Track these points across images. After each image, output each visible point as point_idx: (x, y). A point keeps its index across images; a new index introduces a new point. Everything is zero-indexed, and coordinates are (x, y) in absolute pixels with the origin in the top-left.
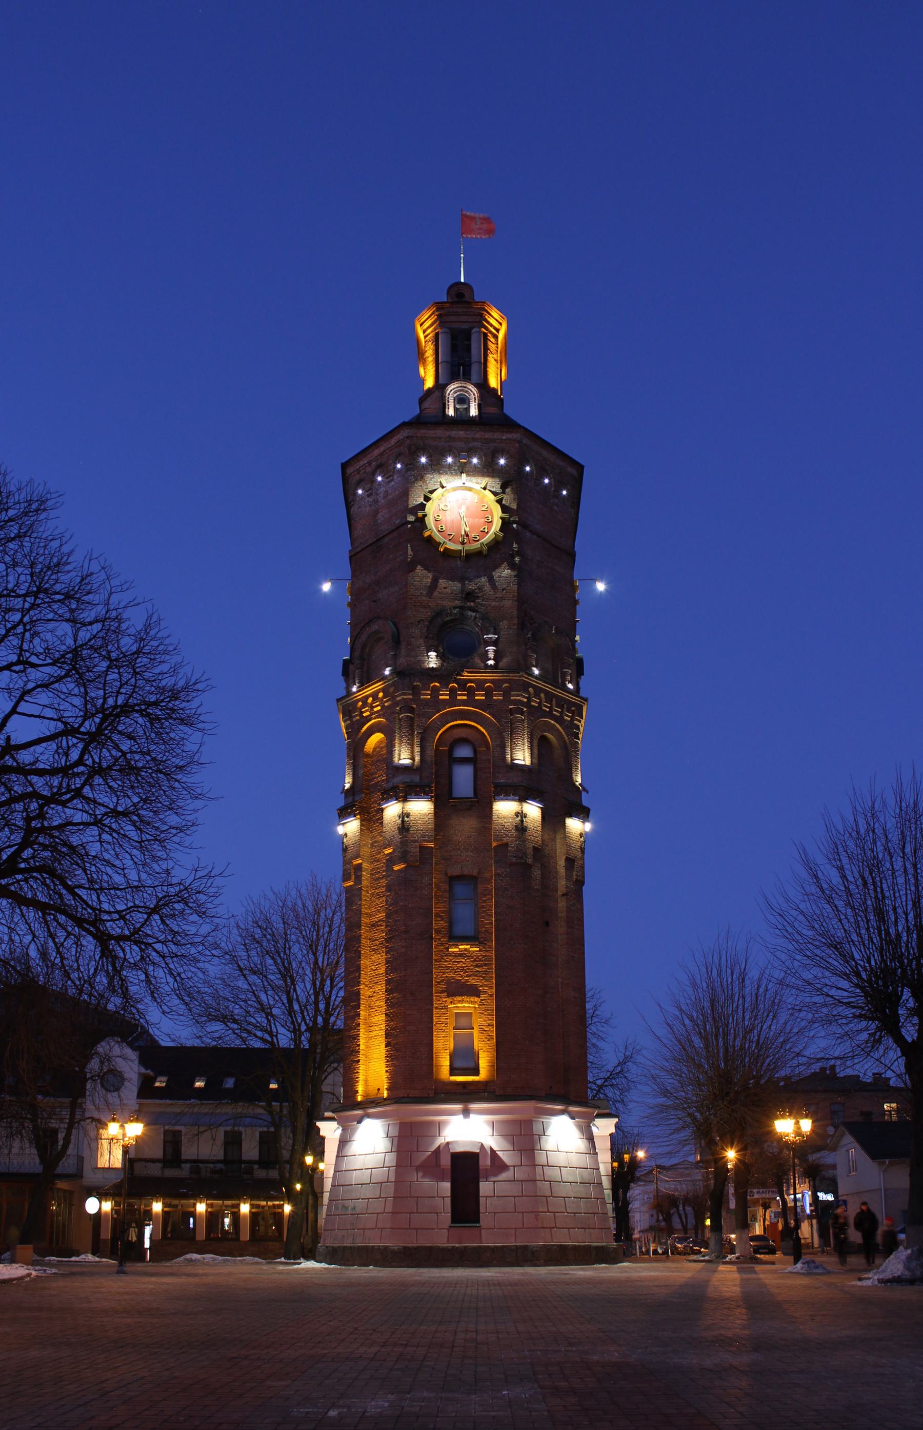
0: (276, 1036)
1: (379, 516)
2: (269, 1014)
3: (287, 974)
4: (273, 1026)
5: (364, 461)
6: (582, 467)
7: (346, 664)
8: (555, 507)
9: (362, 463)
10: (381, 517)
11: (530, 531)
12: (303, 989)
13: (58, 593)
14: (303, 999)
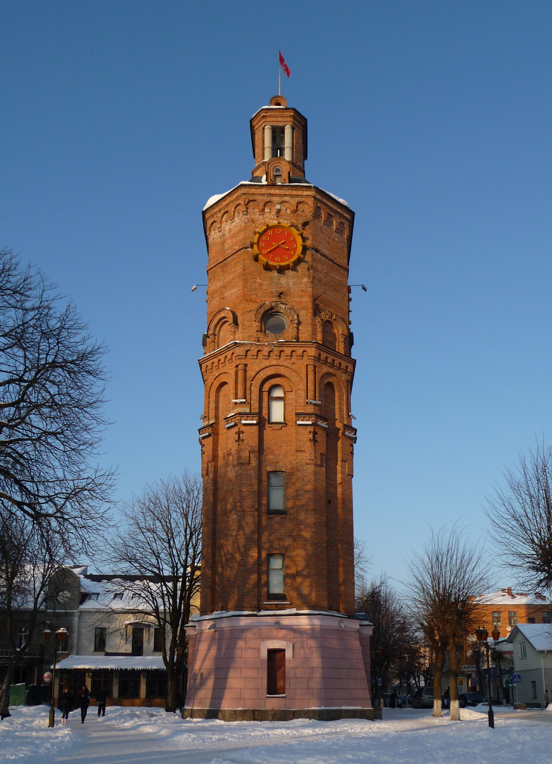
0: (162, 571)
1: (226, 244)
2: (158, 557)
3: (169, 531)
4: (160, 564)
5: (217, 209)
6: (354, 213)
7: (206, 337)
8: (336, 239)
9: (215, 211)
10: (226, 246)
11: (320, 254)
12: (179, 541)
13: (9, 289)
14: (178, 546)
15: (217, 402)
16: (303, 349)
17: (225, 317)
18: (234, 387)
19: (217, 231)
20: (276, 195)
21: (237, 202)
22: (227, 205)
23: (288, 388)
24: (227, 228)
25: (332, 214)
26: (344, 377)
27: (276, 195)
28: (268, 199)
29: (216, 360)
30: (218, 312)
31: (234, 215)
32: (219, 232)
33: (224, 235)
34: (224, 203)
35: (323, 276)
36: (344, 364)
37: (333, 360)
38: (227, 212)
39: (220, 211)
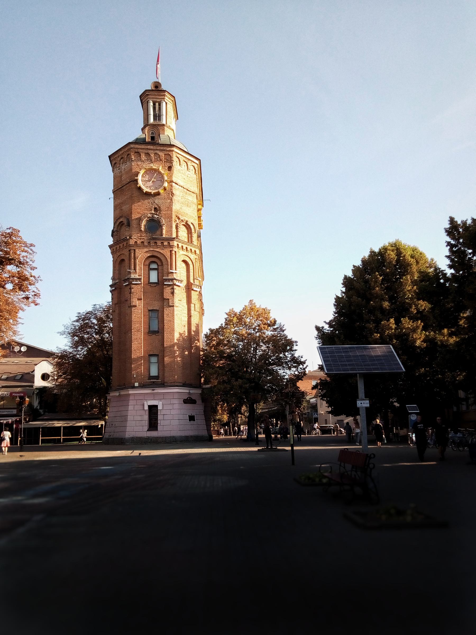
8: (189, 176)
15: (120, 270)
16: (168, 241)
17: (122, 222)
18: (128, 262)
19: (117, 169)
20: (151, 149)
21: (128, 153)
22: (123, 154)
23: (159, 264)
24: (123, 167)
25: (186, 160)
26: (193, 256)
27: (151, 149)
28: (146, 151)
29: (118, 246)
30: (119, 218)
31: (126, 160)
32: (119, 169)
33: (121, 172)
34: (121, 152)
35: (180, 198)
36: (193, 249)
37: (187, 248)
38: (122, 158)
39: (119, 156)
